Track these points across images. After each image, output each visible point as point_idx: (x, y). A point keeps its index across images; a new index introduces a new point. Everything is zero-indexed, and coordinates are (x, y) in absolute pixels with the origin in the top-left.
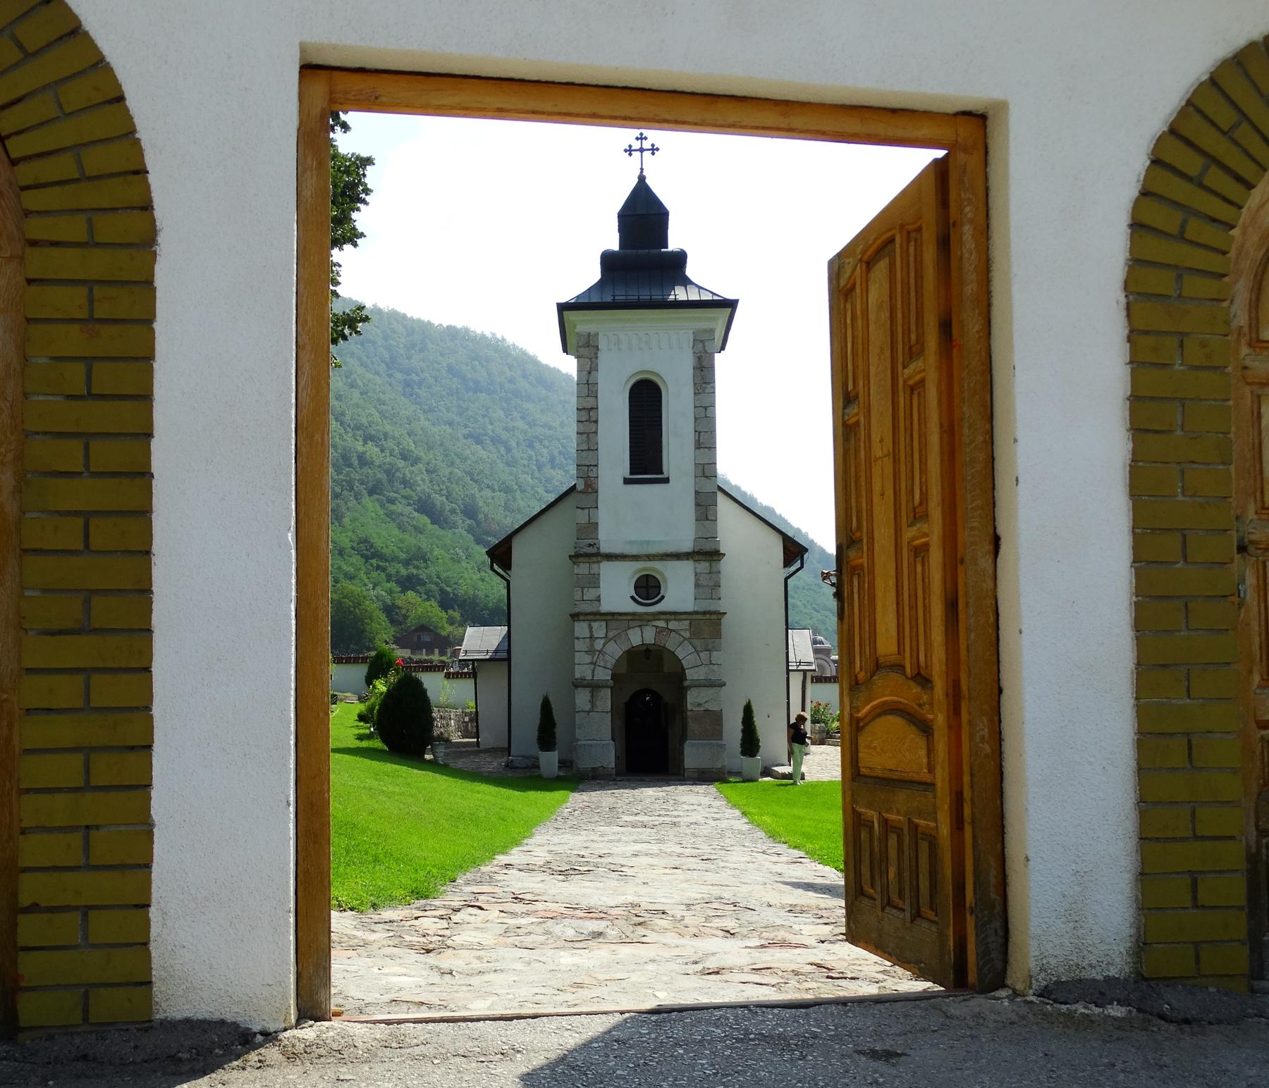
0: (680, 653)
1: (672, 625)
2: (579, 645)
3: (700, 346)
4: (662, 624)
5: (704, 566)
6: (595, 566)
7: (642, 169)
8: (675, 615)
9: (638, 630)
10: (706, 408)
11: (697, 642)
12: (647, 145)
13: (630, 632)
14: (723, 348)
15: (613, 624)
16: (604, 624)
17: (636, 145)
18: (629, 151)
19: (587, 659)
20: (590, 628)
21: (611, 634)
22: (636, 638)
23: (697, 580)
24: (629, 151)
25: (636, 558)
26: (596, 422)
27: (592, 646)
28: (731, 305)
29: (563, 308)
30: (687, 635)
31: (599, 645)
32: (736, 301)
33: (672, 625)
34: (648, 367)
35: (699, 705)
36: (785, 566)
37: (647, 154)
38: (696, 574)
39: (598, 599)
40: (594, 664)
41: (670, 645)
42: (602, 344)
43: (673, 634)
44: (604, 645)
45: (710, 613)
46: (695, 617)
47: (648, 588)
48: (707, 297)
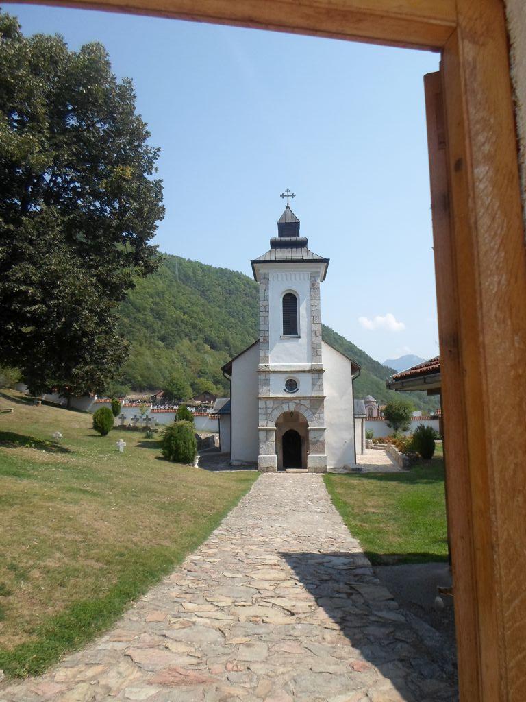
0: (306, 415)
1: (302, 402)
2: (260, 411)
3: (313, 279)
4: (297, 401)
5: (316, 376)
6: (267, 376)
8: (304, 398)
12: (290, 193)
14: (324, 279)
15: (275, 402)
17: (286, 194)
18: (283, 196)
19: (264, 417)
20: (266, 403)
22: (286, 408)
24: (283, 196)
26: (268, 312)
28: (327, 261)
29: (253, 262)
30: (309, 406)
31: (269, 411)
32: (329, 259)
33: (302, 402)
34: (294, 288)
36: (352, 374)
37: (290, 198)
41: (301, 412)
42: (271, 279)
47: (291, 385)
48: (316, 258)
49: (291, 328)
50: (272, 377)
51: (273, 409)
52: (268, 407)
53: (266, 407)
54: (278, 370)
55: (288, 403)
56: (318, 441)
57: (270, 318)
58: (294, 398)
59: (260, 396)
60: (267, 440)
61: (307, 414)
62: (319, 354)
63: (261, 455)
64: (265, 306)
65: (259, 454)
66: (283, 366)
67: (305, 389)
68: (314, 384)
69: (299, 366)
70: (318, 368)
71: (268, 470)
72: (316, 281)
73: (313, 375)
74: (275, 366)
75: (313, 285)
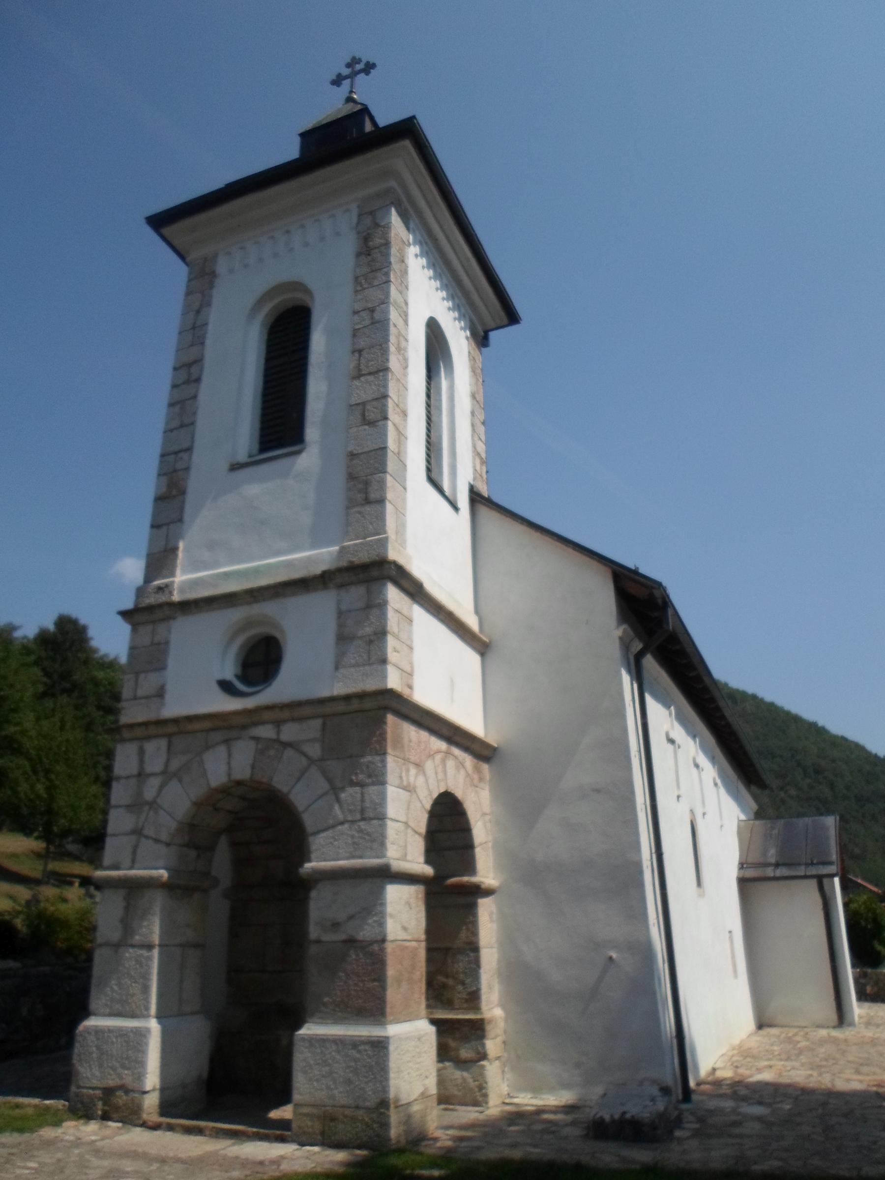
1: (289, 732)
3: (368, 221)
5: (355, 595)
10: (372, 310)
16: (163, 743)
17: (346, 72)
18: (337, 81)
20: (141, 752)
22: (223, 765)
23: (341, 626)
25: (229, 600)
26: (198, 380)
27: (139, 794)
30: (315, 750)
31: (150, 791)
33: (289, 732)
35: (336, 926)
38: (340, 614)
39: (160, 694)
41: (281, 783)
42: (221, 267)
43: (289, 753)
44: (161, 787)
45: (362, 696)
46: (328, 709)
49: (280, 424)
51: (167, 775)
52: (149, 769)
55: (227, 741)
56: (351, 942)
57: (202, 396)
61: (304, 795)
62: (373, 496)
63: (92, 1022)
65: (85, 1012)
66: (227, 575)
67: (309, 671)
68: (343, 638)
69: (289, 564)
70: (364, 557)
71: (116, 1106)
72: (377, 225)
74: (196, 583)
75: (366, 239)
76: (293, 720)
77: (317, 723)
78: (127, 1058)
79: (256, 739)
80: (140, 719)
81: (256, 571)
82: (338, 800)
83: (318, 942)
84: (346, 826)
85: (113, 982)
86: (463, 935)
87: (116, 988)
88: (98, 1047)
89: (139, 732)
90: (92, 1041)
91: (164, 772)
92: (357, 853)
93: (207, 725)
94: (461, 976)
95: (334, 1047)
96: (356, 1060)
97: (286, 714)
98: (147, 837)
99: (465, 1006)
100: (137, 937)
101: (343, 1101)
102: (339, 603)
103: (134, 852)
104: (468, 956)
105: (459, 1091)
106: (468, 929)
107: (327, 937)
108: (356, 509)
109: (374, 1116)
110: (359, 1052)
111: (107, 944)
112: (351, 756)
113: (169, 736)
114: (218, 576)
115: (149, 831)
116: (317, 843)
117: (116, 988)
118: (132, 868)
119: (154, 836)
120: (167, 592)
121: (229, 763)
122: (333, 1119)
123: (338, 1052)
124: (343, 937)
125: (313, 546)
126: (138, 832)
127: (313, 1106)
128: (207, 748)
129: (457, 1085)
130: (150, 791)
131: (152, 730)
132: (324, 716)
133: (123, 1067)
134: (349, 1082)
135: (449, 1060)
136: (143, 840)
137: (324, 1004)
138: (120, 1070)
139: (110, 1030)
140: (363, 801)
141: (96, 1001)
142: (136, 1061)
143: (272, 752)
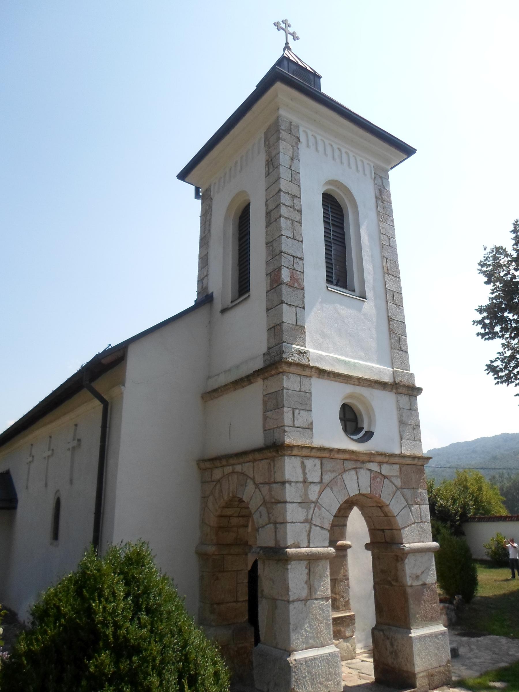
1: (386, 470)
3: (380, 180)
5: (404, 400)
6: (305, 381)
7: (287, 43)
9: (353, 472)
11: (408, 493)
13: (346, 476)
15: (329, 465)
16: (317, 462)
20: (303, 466)
21: (327, 478)
24: (276, 24)
26: (300, 211)
27: (306, 495)
30: (398, 482)
31: (313, 492)
33: (386, 470)
35: (417, 577)
38: (399, 409)
39: (310, 428)
40: (308, 521)
41: (385, 498)
42: (302, 138)
49: (340, 273)
50: (318, 387)
53: (305, 482)
54: (328, 368)
55: (355, 469)
56: (424, 584)
58: (371, 457)
59: (288, 440)
60: (310, 597)
62: (403, 348)
64: (294, 196)
73: (399, 398)
74: (321, 358)
76: (387, 463)
77: (397, 467)
78: (330, 674)
79: (371, 471)
80: (299, 444)
81: (355, 366)
82: (411, 510)
83: (411, 586)
84: (416, 524)
85: (306, 626)
86: (342, 571)
87: (308, 629)
88: (308, 672)
89: (305, 452)
90: (305, 669)
91: (321, 482)
92: (422, 540)
93: (347, 456)
94: (342, 593)
95: (429, 639)
96: (437, 644)
97: (386, 459)
98: (315, 525)
99: (344, 608)
100: (318, 593)
101: (435, 665)
102: (398, 401)
103: (309, 535)
104: (345, 583)
105: (346, 653)
106: (344, 568)
107: (414, 584)
108: (396, 351)
109: (446, 668)
110: (438, 639)
111: (298, 600)
112: (413, 488)
113: (321, 458)
114: (333, 358)
115: (316, 521)
116: (406, 533)
117: (308, 629)
118: (308, 547)
119: (320, 525)
120: (305, 357)
121: (358, 482)
122: (432, 675)
123: (430, 641)
124: (421, 583)
125: (379, 363)
126: (308, 521)
127: (424, 671)
128: (345, 471)
129: (345, 651)
130: (313, 492)
131: (314, 453)
132: (400, 464)
133: (327, 680)
134: (436, 655)
135: (341, 639)
136: (313, 527)
137: (417, 619)
138: (325, 683)
139: (315, 658)
140: (420, 512)
141: (295, 639)
142: (336, 674)
143: (379, 480)
